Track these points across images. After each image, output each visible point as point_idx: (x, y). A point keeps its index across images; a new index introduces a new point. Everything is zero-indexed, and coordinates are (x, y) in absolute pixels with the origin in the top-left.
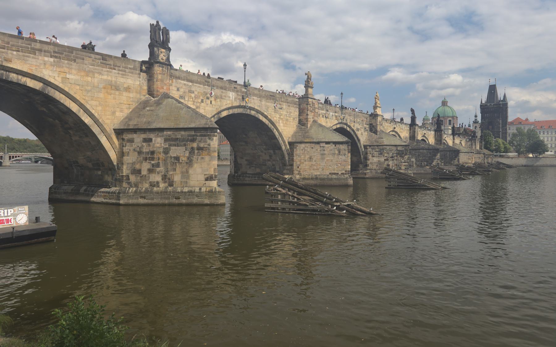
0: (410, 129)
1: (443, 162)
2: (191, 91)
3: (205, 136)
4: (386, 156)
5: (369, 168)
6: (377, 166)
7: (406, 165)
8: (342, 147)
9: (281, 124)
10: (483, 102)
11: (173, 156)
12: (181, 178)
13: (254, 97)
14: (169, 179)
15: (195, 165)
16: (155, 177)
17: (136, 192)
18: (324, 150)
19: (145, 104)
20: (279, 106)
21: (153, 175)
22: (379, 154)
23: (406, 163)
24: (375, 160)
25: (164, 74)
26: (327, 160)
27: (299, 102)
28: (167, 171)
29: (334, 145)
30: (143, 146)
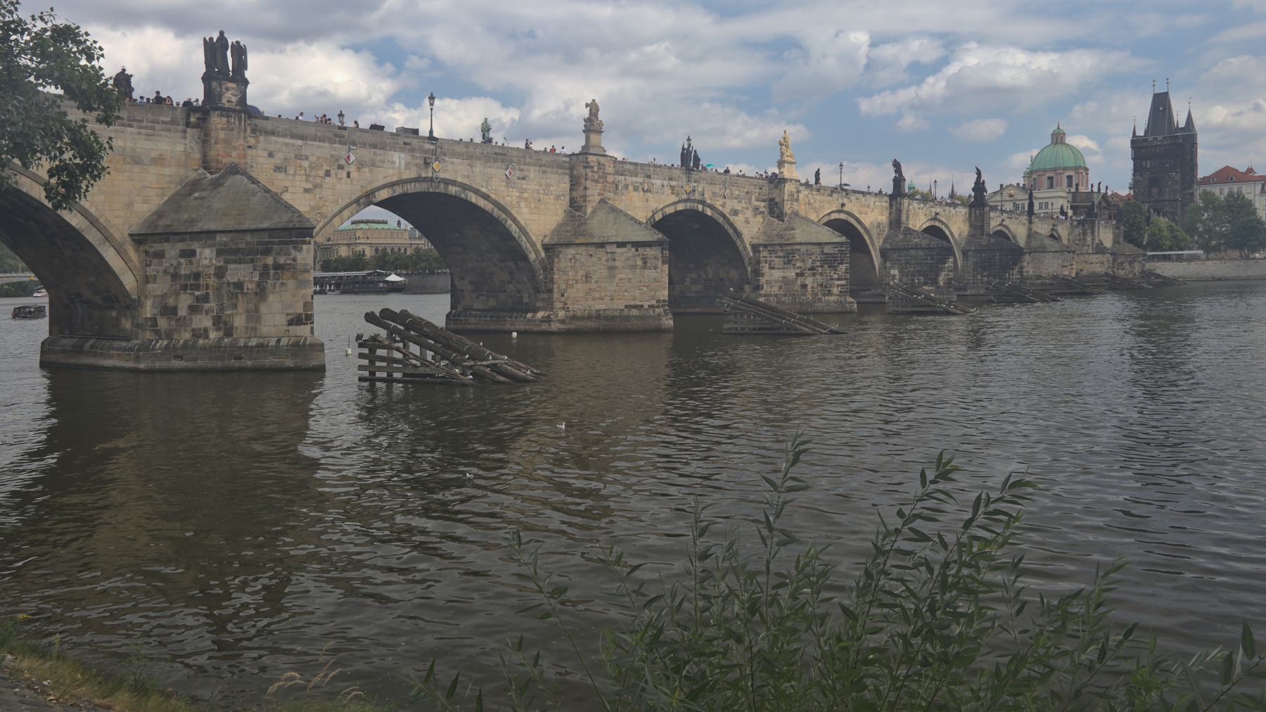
0: (891, 205)
1: (985, 276)
2: (301, 155)
3: (287, 243)
4: (800, 268)
5: (763, 292)
6: (780, 288)
7: (842, 285)
8: (650, 252)
9: (525, 210)
10: (1140, 133)
11: (232, 281)
12: (247, 322)
13: (454, 160)
15: (271, 298)
16: (200, 320)
17: (167, 347)
18: (614, 260)
19: (194, 186)
20: (518, 173)
21: (199, 316)
22: (784, 263)
23: (842, 280)
24: (777, 274)
25: (232, 129)
26: (620, 279)
28: (222, 310)
29: (634, 250)
30: (180, 264)
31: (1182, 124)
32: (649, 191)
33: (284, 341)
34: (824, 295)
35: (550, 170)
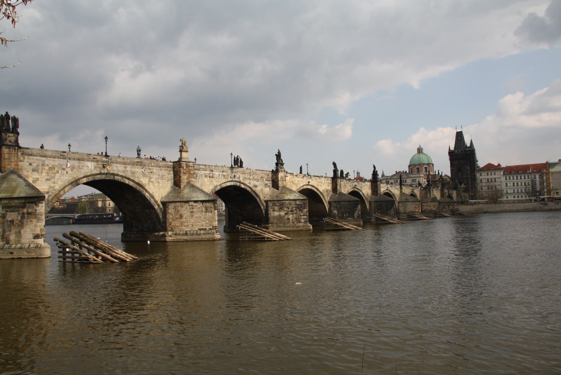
0: (332, 182)
1: (379, 213)
3: (32, 203)
4: (286, 211)
7: (305, 218)
10: (452, 148)
13: (117, 165)
14: (6, 238)
18: (193, 208)
20: (148, 171)
22: (279, 209)
23: (305, 216)
24: (276, 214)
26: (196, 217)
27: (173, 165)
29: (201, 204)
31: (468, 145)
32: (212, 177)
33: (32, 245)
34: (298, 223)
35: (164, 168)
